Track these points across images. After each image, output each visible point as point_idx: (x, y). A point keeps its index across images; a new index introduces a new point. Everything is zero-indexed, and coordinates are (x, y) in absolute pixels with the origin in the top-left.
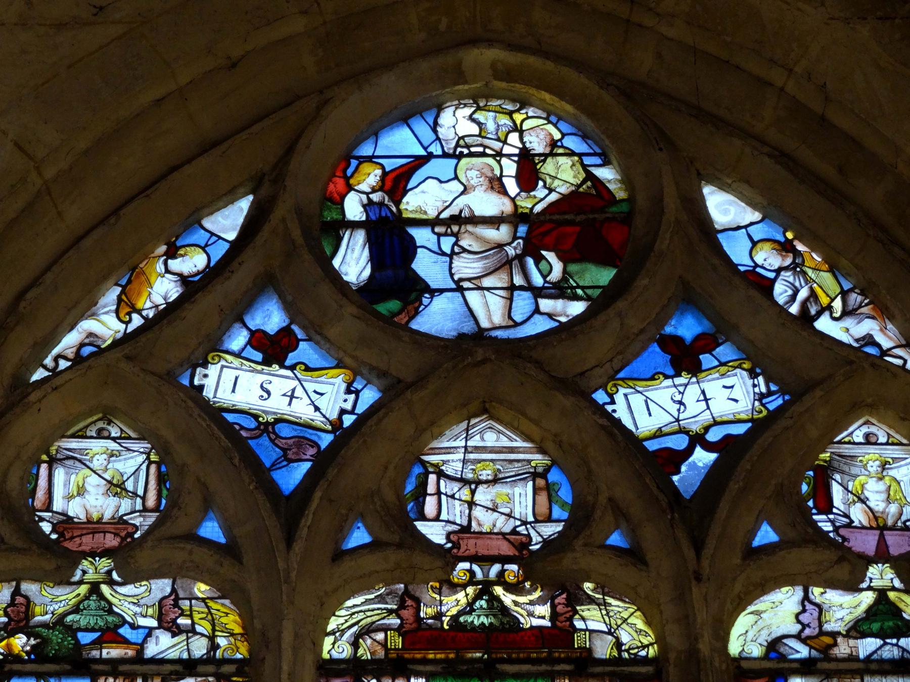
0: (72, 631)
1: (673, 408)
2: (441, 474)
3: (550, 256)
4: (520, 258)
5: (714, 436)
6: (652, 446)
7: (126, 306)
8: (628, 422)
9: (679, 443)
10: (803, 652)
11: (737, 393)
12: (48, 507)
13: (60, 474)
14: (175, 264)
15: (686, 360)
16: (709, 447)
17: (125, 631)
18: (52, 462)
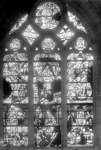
0: (14, 58)
1: (64, 36)
2: (44, 43)
3: (54, 20)
4: (51, 20)
5: (67, 39)
6: (62, 40)
7: (17, 26)
8: (60, 37)
9: (64, 39)
10: (73, 59)
11: (70, 34)
12: (11, 47)
13: (12, 44)
14: (21, 22)
15: (65, 30)
16: (67, 40)
17: (18, 58)
18: (11, 43)
